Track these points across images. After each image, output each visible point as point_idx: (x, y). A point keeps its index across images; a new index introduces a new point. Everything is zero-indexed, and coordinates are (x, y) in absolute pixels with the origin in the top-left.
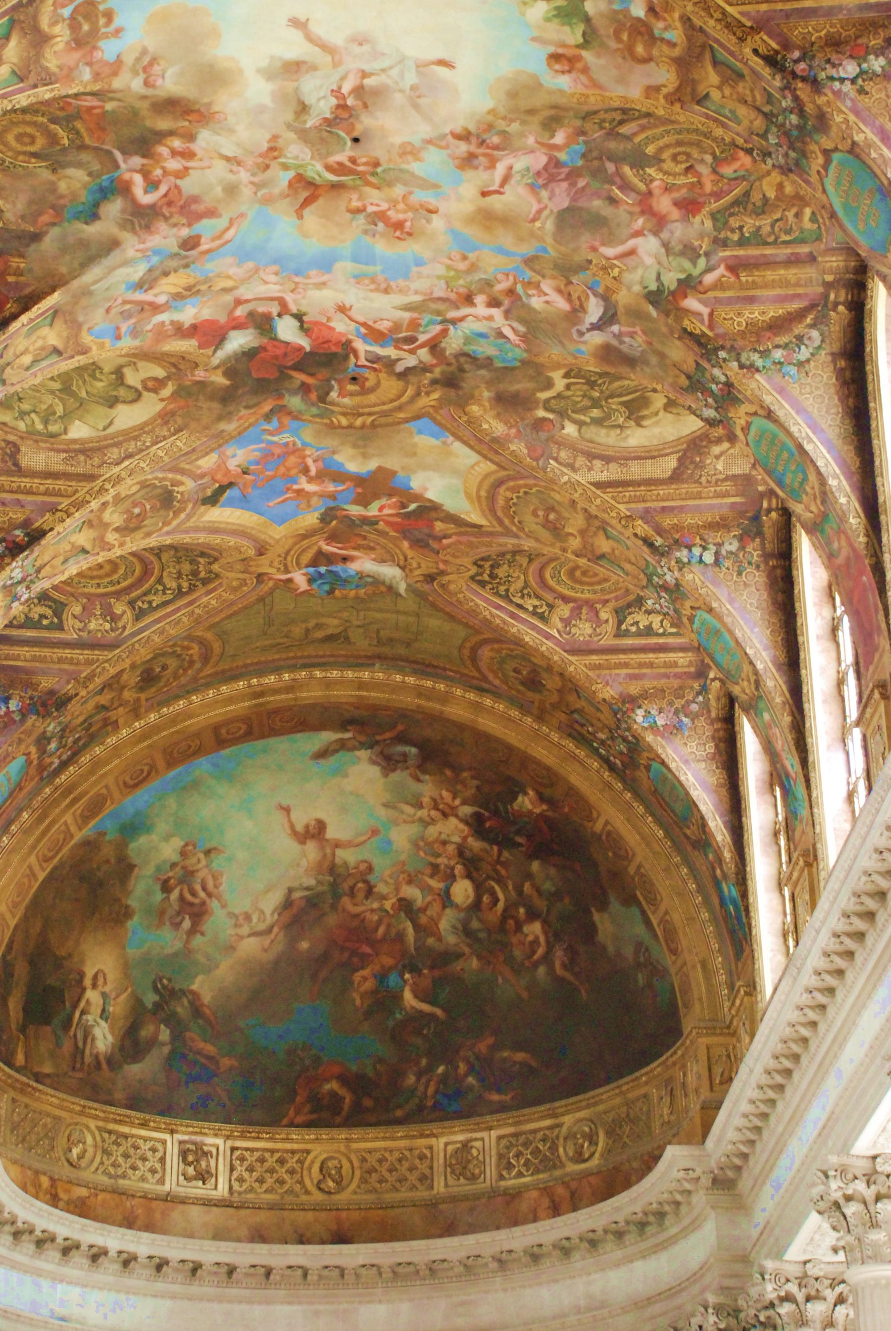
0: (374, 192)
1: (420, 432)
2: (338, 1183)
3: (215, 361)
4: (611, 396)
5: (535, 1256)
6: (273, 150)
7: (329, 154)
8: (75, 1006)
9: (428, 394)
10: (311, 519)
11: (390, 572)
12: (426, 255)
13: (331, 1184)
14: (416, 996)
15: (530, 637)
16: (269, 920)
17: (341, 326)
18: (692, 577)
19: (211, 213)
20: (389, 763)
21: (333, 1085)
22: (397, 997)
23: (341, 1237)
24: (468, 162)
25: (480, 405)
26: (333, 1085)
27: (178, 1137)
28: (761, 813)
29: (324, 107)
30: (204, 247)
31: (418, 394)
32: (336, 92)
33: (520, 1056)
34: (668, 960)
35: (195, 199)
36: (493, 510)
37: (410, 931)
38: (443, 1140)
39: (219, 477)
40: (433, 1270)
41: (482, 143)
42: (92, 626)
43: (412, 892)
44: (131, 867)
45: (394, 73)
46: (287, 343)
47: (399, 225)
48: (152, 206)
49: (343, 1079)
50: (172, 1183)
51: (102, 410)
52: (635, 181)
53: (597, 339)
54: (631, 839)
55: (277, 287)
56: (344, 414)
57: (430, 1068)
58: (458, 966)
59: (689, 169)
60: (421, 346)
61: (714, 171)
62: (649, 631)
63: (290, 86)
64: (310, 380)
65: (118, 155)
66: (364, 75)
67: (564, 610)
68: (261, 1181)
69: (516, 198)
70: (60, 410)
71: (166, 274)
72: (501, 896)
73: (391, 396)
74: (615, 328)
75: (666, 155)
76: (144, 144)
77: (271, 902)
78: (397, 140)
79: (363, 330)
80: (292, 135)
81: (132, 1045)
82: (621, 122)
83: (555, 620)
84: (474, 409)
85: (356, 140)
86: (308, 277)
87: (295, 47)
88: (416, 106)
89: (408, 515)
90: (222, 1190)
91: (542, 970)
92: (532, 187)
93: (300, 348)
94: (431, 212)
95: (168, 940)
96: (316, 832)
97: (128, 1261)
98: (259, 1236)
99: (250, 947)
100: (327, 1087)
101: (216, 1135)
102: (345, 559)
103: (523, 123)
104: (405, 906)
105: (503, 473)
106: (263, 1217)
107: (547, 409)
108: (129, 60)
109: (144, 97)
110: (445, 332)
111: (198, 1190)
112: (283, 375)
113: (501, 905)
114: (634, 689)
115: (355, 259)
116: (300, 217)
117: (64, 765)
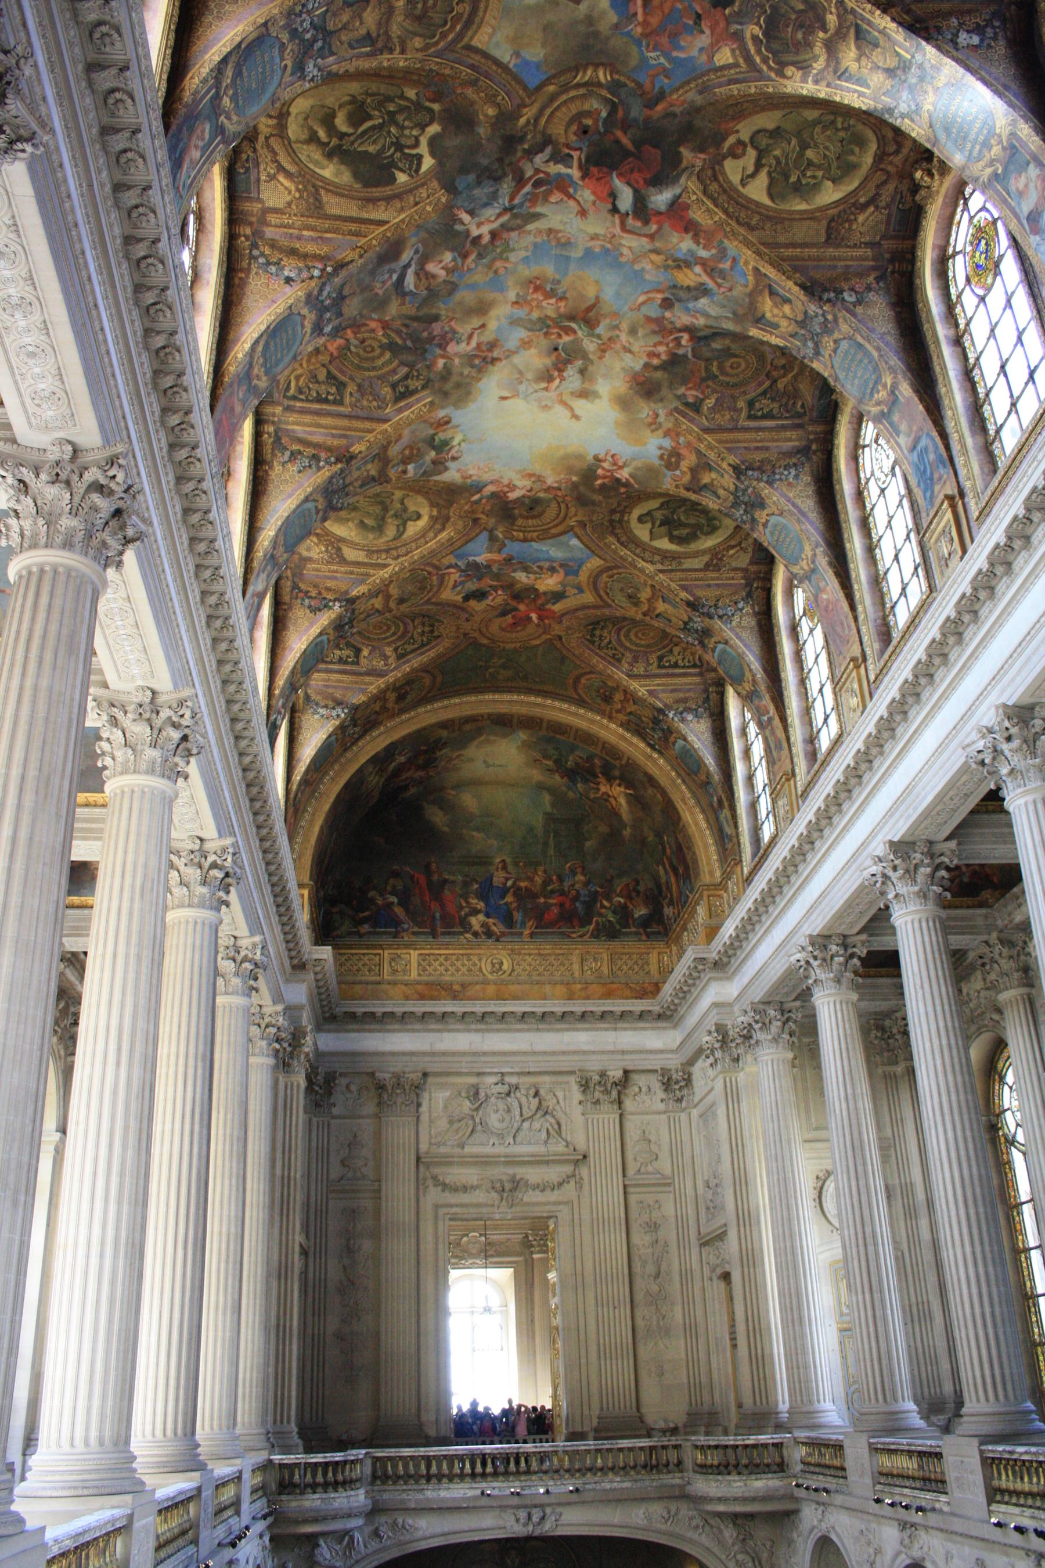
0: (551, 313)
1: (538, 66)
3: (683, 180)
4: (380, 127)
6: (603, 350)
7: (573, 342)
9: (528, 122)
12: (520, 267)
17: (586, 195)
19: (649, 319)
24: (492, 345)
25: (486, 116)
29: (571, 372)
30: (660, 296)
31: (537, 120)
32: (562, 379)
35: (654, 332)
39: (722, 24)
41: (484, 359)
45: (531, 390)
46: (629, 184)
47: (537, 289)
48: (680, 331)
51: (789, 126)
52: (393, 335)
53: (405, 257)
55: (624, 242)
56: (599, 85)
59: (363, 341)
60: (530, 178)
61: (347, 340)
63: (586, 385)
64: (619, 134)
65: (690, 355)
66: (546, 389)
69: (463, 329)
70: (818, 129)
71: (688, 288)
73: (558, 114)
74: (395, 277)
75: (378, 351)
76: (674, 361)
78: (533, 351)
79: (571, 191)
80: (591, 356)
82: (406, 377)
84: (491, 112)
85: (556, 349)
86: (602, 246)
87: (581, 405)
88: (520, 373)
92: (455, 332)
93: (619, 175)
94: (516, 303)
103: (461, 374)
105: (466, 40)
107: (430, 111)
108: (660, 432)
109: (661, 400)
110: (512, 199)
112: (638, 143)
115: (568, 258)
116: (597, 298)
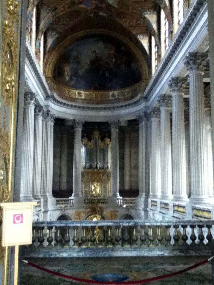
5: (122, 106)
10: (94, 7)
11: (104, 15)
15: (124, 25)
16: (88, 63)
18: (147, 16)
20: (104, 42)
21: (96, 85)
23: (98, 104)
27: (78, 91)
28: (154, 50)
34: (141, 70)
36: (119, 5)
37: (107, 66)
40: (109, 108)
42: (64, 22)
43: (107, 60)
44: (70, 56)
50: (77, 96)
54: (137, 53)
62: (140, 24)
67: (129, 21)
68: (88, 97)
72: (119, 61)
77: (88, 61)
81: (71, 79)
83: (127, 22)
89: (107, 6)
90: (83, 97)
95: (75, 66)
96: (95, 52)
97: (72, 106)
98: (88, 103)
99: (86, 67)
101: (82, 91)
102: (99, 13)
104: (106, 62)
106: (87, 101)
111: (80, 97)
113: (119, 62)
114: (138, 32)
117: (61, 42)
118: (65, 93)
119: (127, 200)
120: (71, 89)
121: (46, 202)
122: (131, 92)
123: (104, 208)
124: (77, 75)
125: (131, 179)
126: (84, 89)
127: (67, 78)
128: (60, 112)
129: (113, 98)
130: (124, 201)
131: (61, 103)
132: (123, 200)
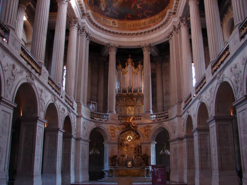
2: (130, 26)
5: (152, 30)
8: (100, 4)
13: (129, 26)
14: (139, 6)
21: (130, 16)
22: (137, 7)
26: (130, 16)
33: (151, 12)
38: (142, 22)
40: (141, 33)
49: (131, 16)
57: (141, 14)
58: (144, 3)
68: (121, 26)
81: (106, 10)
90: (117, 26)
91: (153, 2)
98: (121, 30)
100: (129, 17)
101: (116, 20)
118: (101, 20)
119: (159, 114)
120: (105, 17)
121: (79, 108)
122: (160, 18)
123: (138, 124)
124: (112, 7)
125: (163, 104)
126: (117, 19)
127: (103, 9)
128: (96, 35)
129: (144, 26)
130: (157, 116)
131: (96, 26)
132: (156, 115)
